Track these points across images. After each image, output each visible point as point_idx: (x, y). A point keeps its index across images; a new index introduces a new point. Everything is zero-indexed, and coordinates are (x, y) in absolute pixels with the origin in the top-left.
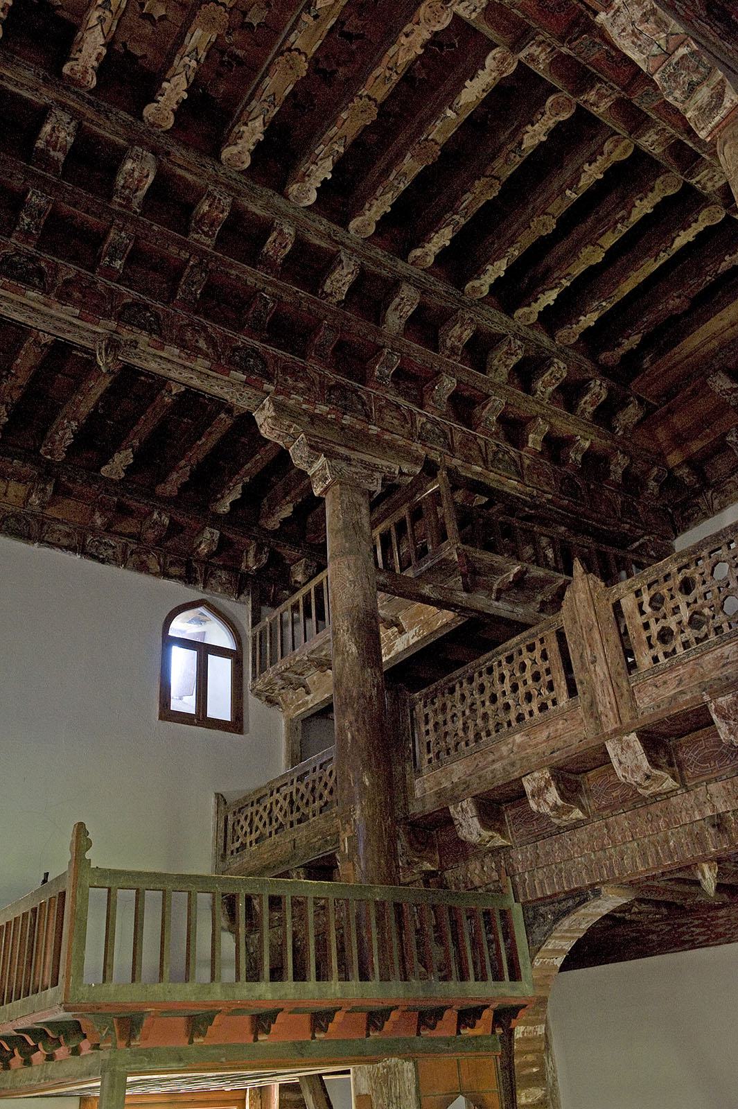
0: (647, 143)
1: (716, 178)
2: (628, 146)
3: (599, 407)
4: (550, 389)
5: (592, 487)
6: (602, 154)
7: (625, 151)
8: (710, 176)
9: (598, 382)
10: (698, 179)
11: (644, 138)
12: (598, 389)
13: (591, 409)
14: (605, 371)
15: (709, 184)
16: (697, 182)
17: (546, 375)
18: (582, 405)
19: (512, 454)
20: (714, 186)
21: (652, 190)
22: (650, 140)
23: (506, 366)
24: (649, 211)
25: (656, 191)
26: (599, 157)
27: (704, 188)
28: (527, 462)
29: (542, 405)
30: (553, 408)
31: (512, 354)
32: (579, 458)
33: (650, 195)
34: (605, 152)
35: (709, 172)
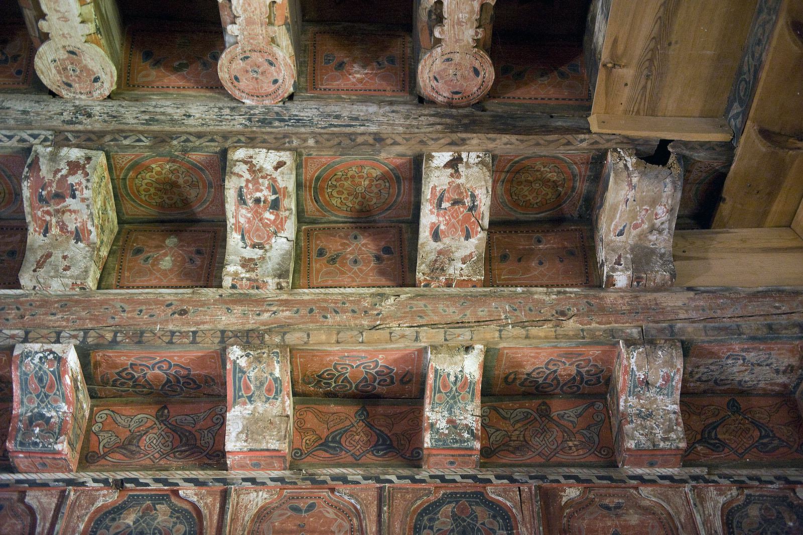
3: (496, 225)
4: (281, 244)
5: (572, 493)
9: (442, 157)
12: (458, 188)
13: (475, 244)
14: (466, 117)
17: (231, 206)
18: (433, 245)
19: (188, 492)
23: (79, 236)
28: (257, 499)
29: (260, 301)
30: (306, 294)
31: (60, 197)
32: (470, 414)
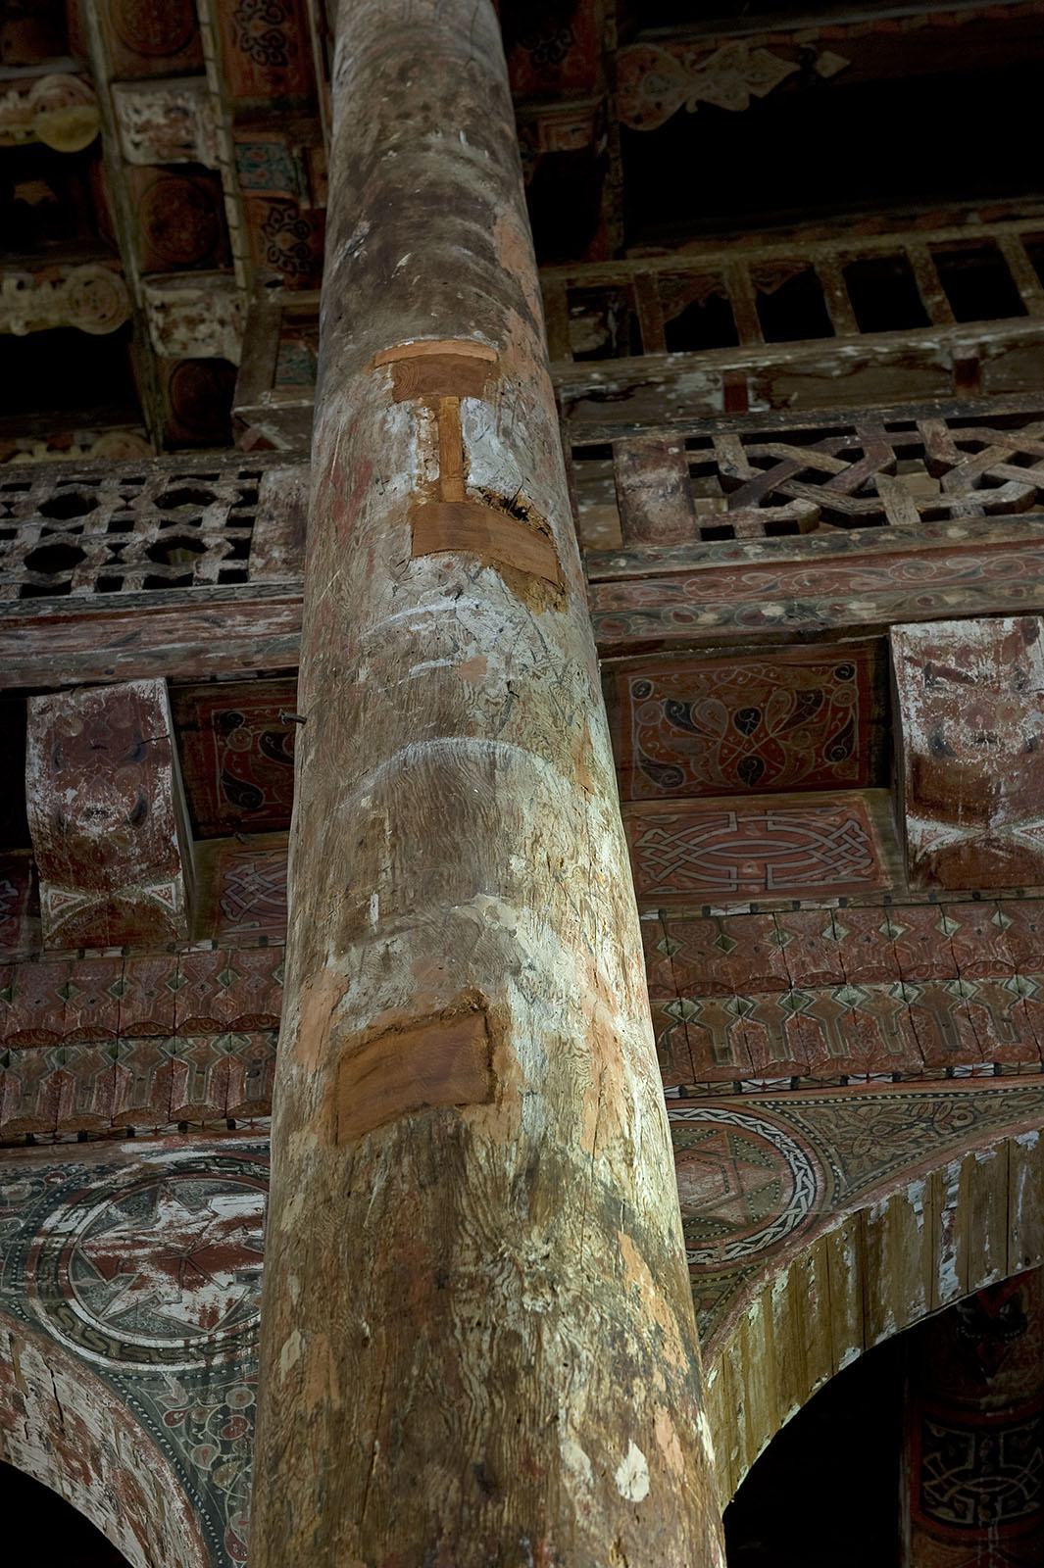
0: (135, 118)
1: (203, 330)
2: (86, 127)
6: (23, 94)
7: (70, 134)
8: (193, 312)
10: (169, 296)
11: (137, 100)
15: (181, 333)
16: (163, 308)
20: (185, 346)
21: (56, 283)
22: (146, 115)
24: (18, 329)
25: (61, 293)
26: (13, 95)
27: (165, 335)
33: (46, 289)
34: (34, 96)
35: (200, 299)
